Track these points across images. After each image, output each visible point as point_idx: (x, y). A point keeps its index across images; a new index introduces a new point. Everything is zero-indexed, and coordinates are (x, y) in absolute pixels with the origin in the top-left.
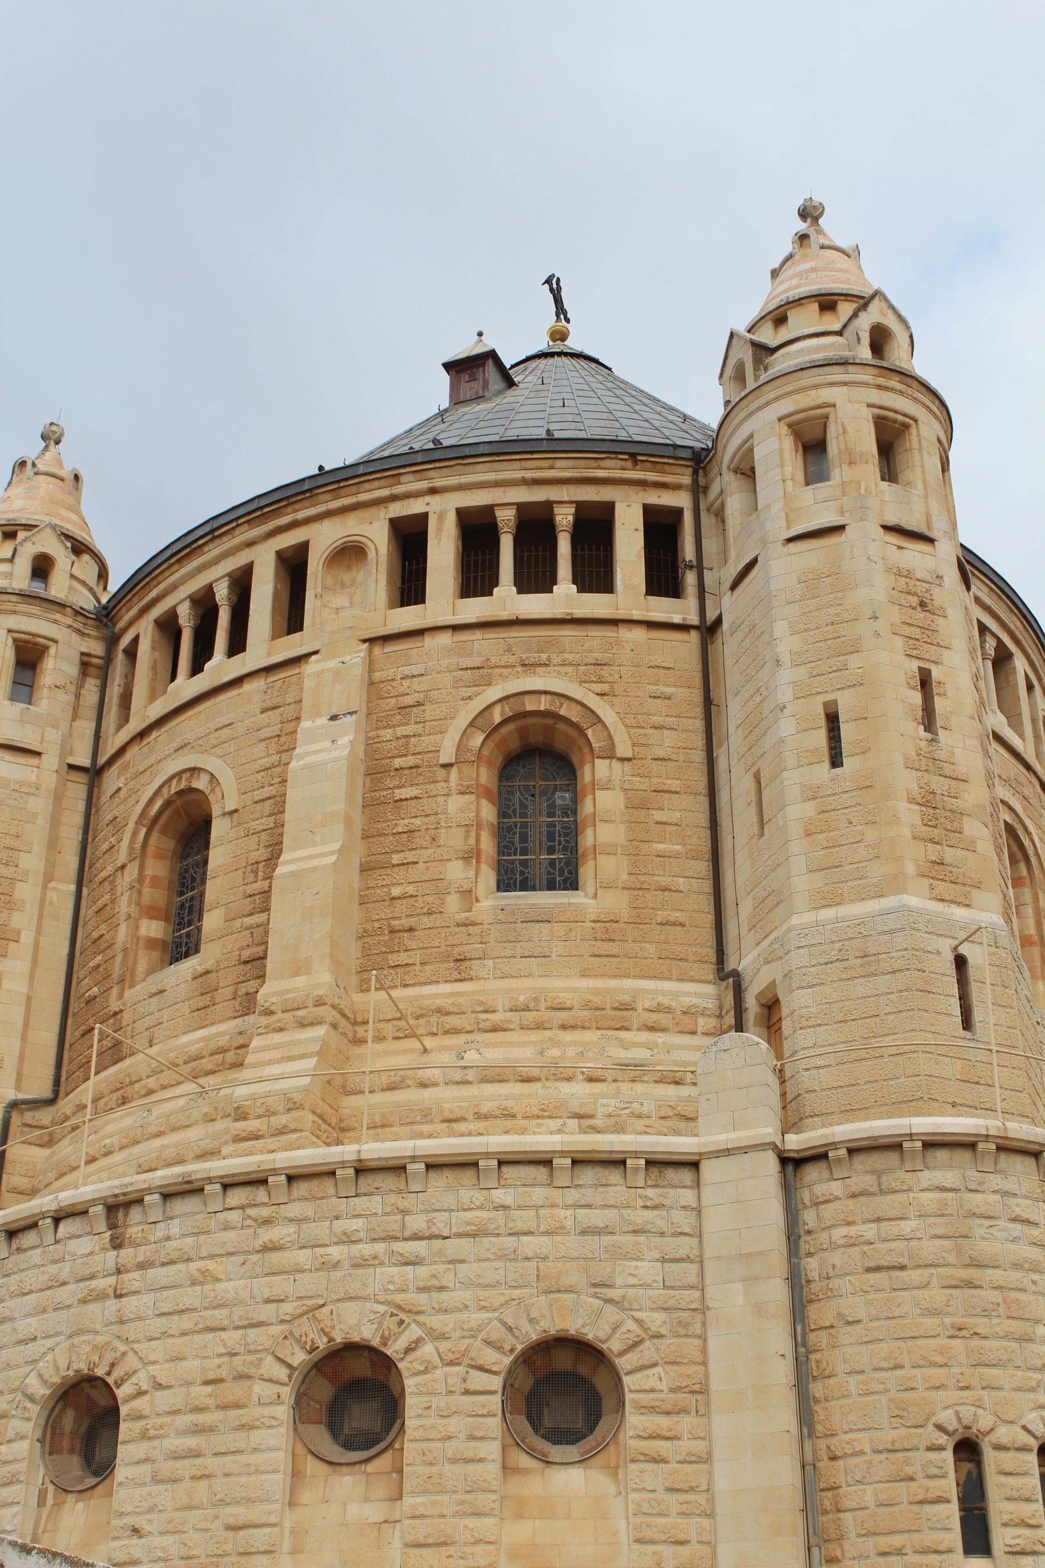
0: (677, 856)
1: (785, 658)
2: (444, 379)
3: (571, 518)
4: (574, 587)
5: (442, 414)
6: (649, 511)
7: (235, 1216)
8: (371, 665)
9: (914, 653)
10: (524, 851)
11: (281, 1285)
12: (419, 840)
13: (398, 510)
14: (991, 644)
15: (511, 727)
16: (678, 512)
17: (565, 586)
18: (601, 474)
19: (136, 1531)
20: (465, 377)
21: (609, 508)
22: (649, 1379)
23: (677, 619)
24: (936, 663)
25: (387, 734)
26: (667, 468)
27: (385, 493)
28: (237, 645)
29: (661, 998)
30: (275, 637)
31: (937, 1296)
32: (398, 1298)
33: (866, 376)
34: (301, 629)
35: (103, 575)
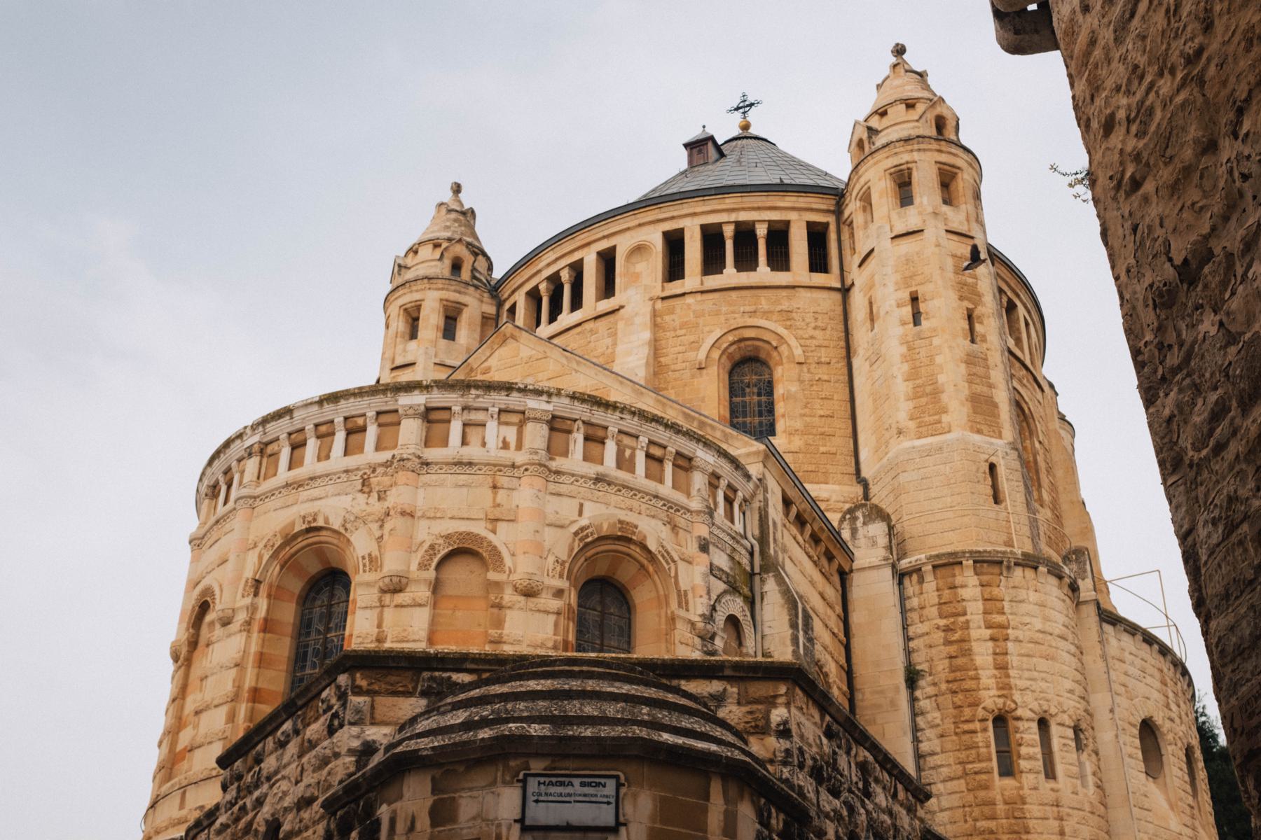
2: (684, 153)
4: (769, 269)
5: (684, 173)
6: (811, 226)
8: (655, 314)
10: (745, 416)
13: (668, 226)
14: (1005, 300)
15: (734, 347)
16: (826, 226)
20: (695, 151)
21: (787, 223)
28: (576, 304)
30: (599, 299)
33: (935, 146)
34: (613, 295)
35: (490, 268)
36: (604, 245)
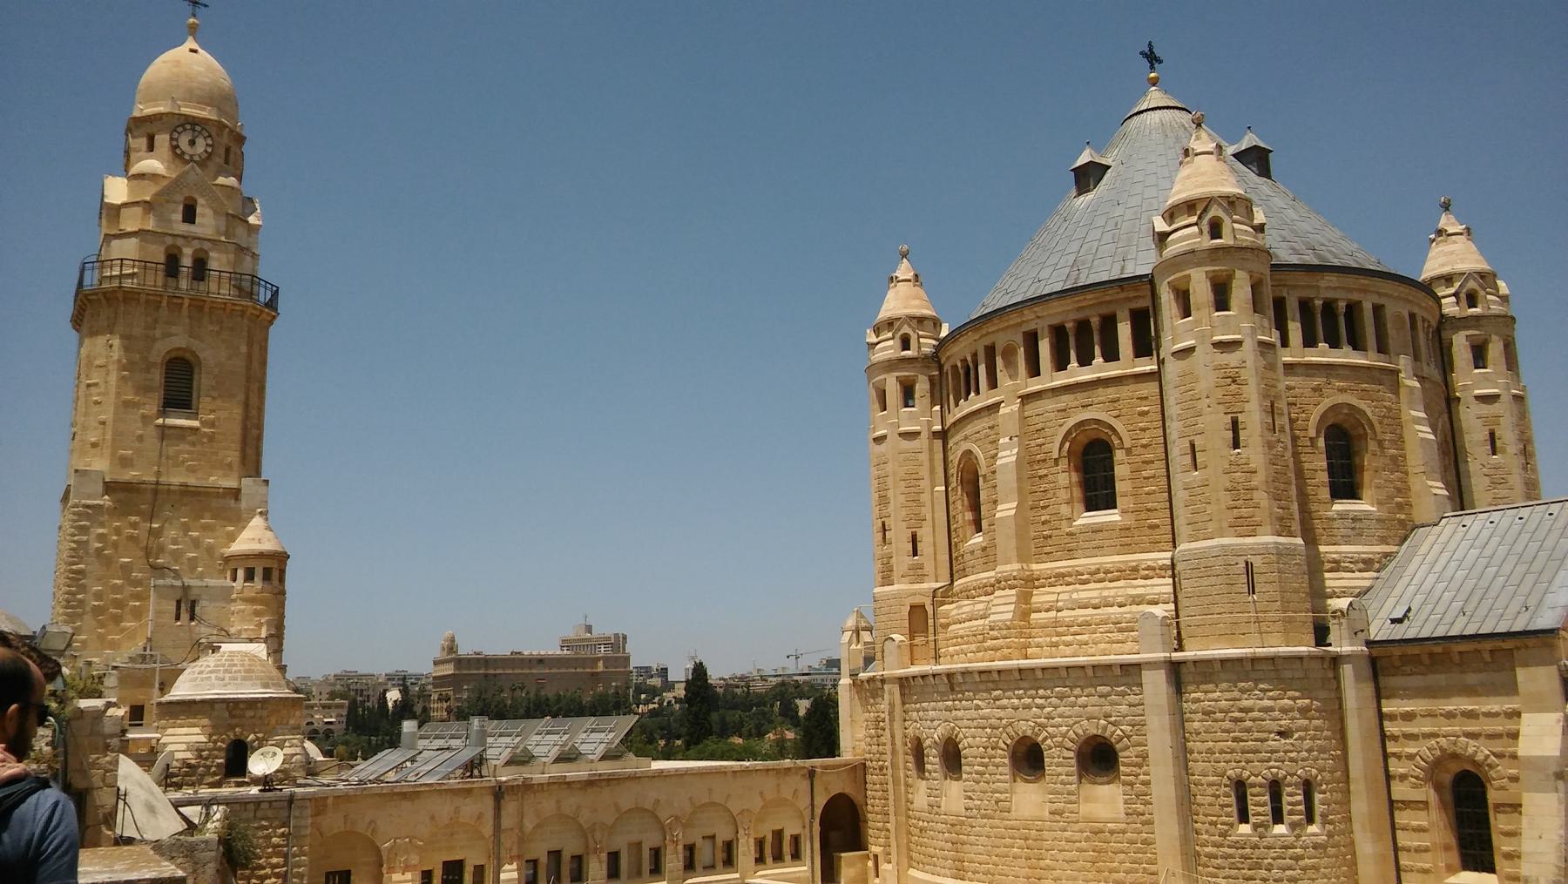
0: (1154, 492)
1: (1175, 417)
2: (1073, 173)
3: (1097, 323)
4: (1101, 360)
7: (982, 687)
8: (1021, 410)
9: (1229, 410)
11: (1001, 713)
12: (1049, 496)
17: (1098, 360)
18: (1108, 298)
19: (971, 798)
22: (1126, 753)
23: (1148, 368)
24: (1241, 412)
25: (1033, 443)
26: (1139, 288)
27: (1019, 320)
28: (978, 392)
29: (1149, 563)
31: (1227, 725)
32: (1038, 720)
36: (987, 341)
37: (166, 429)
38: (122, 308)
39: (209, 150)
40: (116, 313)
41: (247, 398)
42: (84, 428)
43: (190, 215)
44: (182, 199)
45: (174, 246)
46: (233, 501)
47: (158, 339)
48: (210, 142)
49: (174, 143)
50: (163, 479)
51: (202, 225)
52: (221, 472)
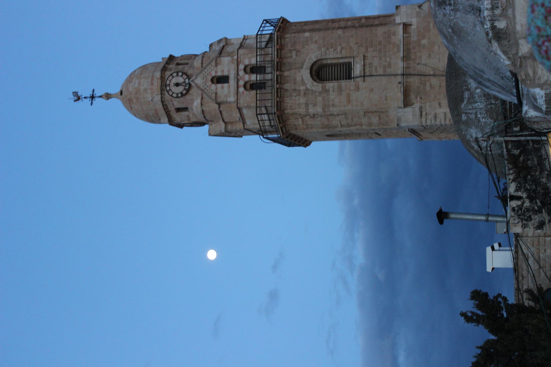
37: (366, 75)
38: (289, 111)
39: (180, 74)
40: (292, 114)
41: (339, 28)
42: (370, 124)
43: (222, 80)
44: (213, 86)
45: (245, 86)
46: (412, 27)
47: (306, 87)
48: (175, 75)
49: (180, 95)
50: (400, 72)
51: (229, 71)
52: (393, 37)
